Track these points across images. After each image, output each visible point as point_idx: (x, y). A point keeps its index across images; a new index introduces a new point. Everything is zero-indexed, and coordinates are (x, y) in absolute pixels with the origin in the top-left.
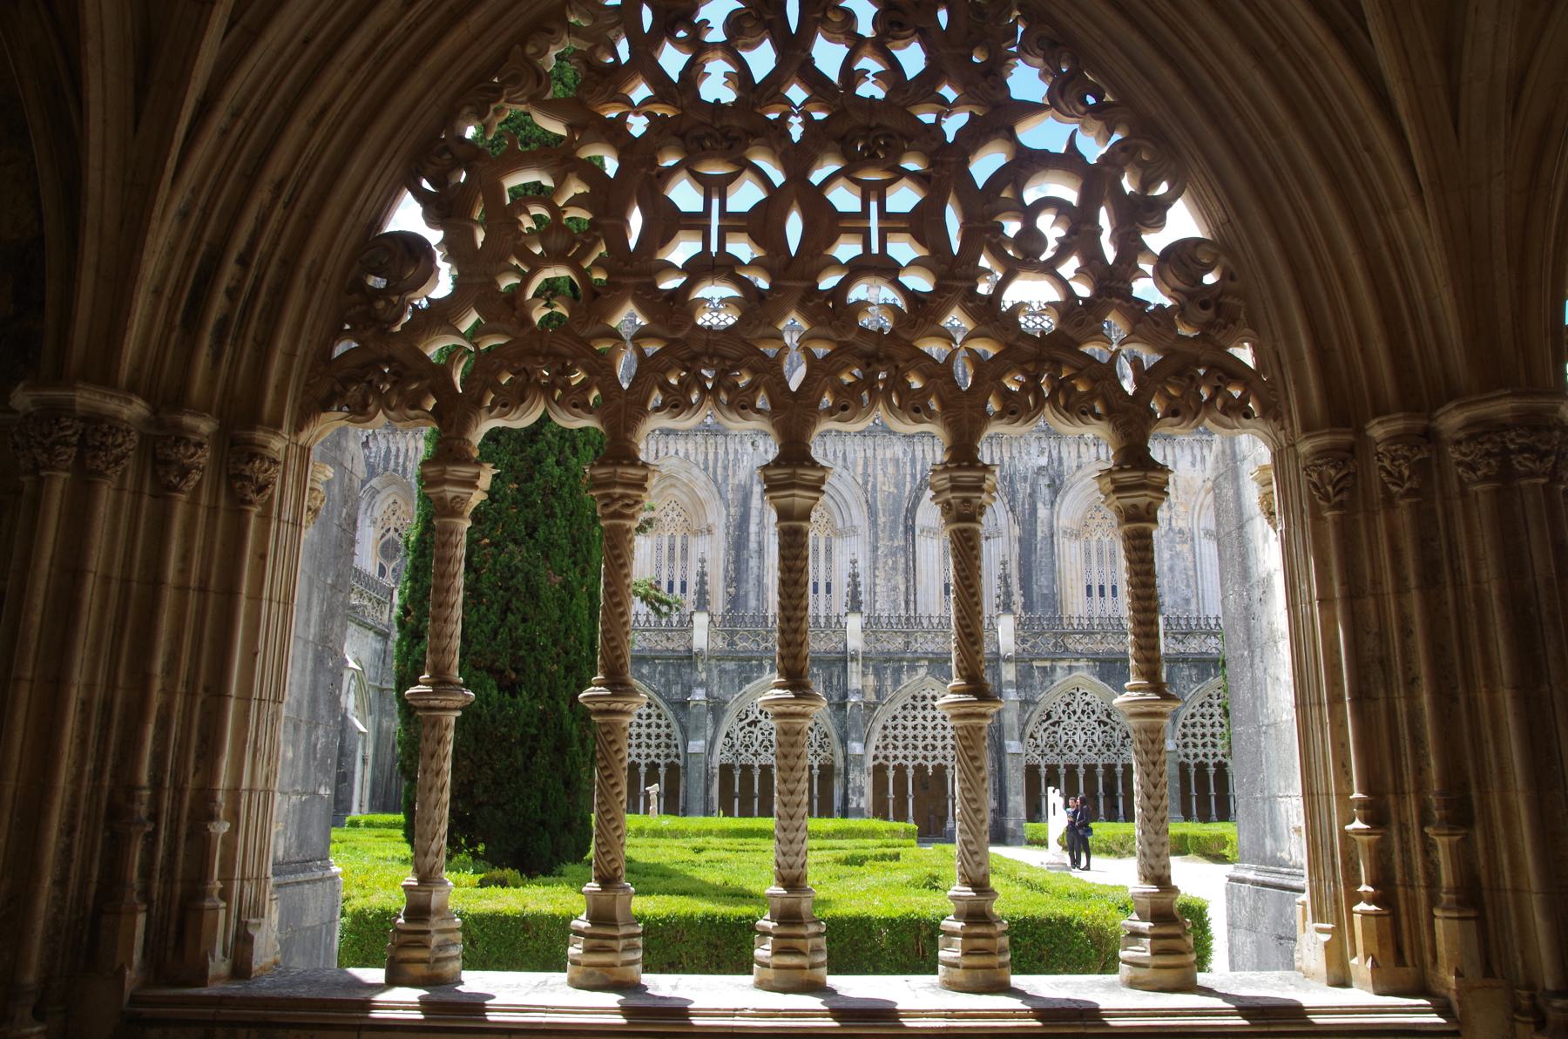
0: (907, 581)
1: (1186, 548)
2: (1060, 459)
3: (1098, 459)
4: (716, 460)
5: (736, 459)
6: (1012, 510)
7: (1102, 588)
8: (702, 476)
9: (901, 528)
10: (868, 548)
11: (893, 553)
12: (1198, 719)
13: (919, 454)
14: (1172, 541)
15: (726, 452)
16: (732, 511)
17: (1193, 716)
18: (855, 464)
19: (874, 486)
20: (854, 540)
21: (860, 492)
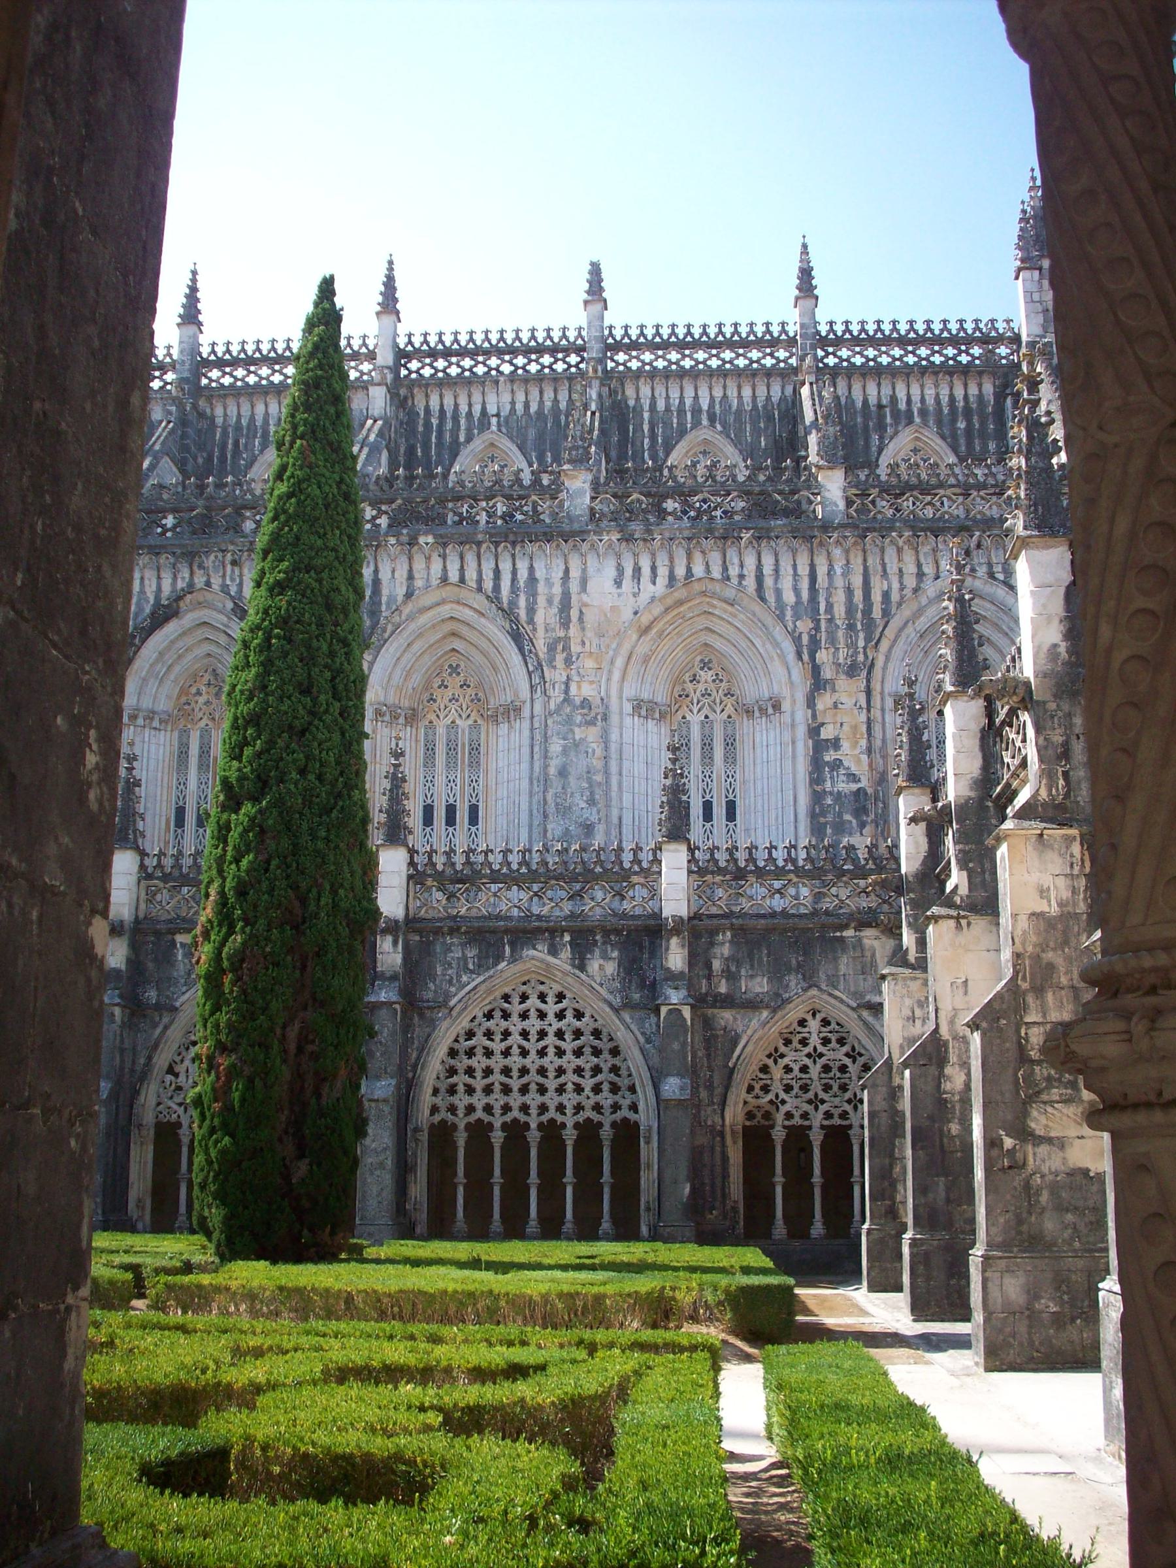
1: (592, 735)
3: (444, 579)
7: (451, 811)
12: (479, 1040)
14: (569, 721)
17: (470, 1034)
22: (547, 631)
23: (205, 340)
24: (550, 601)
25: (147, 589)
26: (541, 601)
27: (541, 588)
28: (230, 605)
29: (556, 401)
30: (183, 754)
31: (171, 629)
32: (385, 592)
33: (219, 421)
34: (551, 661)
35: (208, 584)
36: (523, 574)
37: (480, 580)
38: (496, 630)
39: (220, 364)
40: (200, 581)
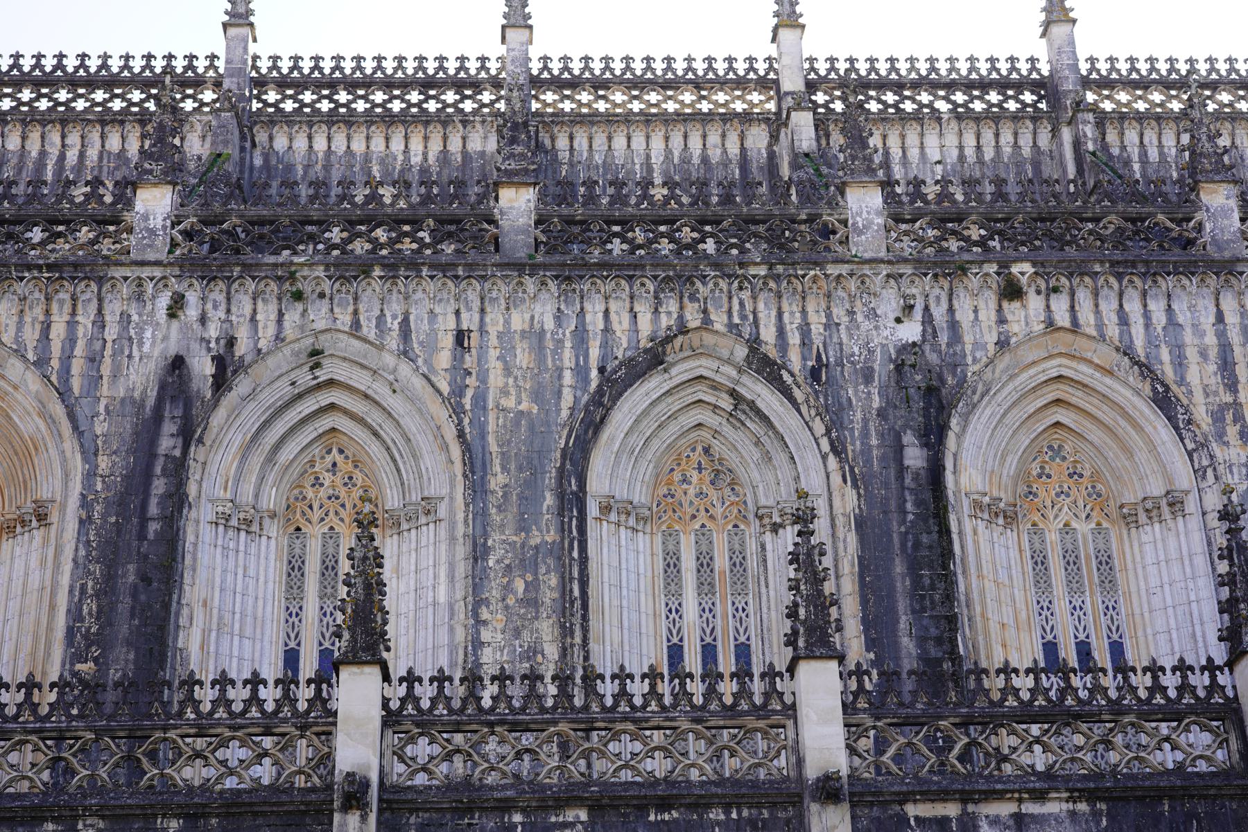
0: (566, 631)
2: (954, 325)
3: (1050, 323)
4: (71, 340)
5: (125, 338)
6: (838, 449)
8: (33, 382)
9: (549, 500)
10: (462, 551)
11: (526, 561)
13: (595, 321)
15: (100, 323)
16: (103, 463)
18: (431, 346)
19: (480, 400)
20: (428, 533)
21: (442, 414)
22: (1207, 395)
23: (535, 52)
24: (1203, 354)
25: (615, 326)
26: (1192, 354)
27: (1188, 337)
28: (741, 352)
29: (1016, 145)
30: (672, 566)
31: (653, 385)
32: (968, 339)
33: (564, 156)
34: (1221, 436)
35: (707, 321)
36: (1159, 318)
37: (1100, 326)
38: (1131, 395)
39: (557, 84)
40: (693, 318)
